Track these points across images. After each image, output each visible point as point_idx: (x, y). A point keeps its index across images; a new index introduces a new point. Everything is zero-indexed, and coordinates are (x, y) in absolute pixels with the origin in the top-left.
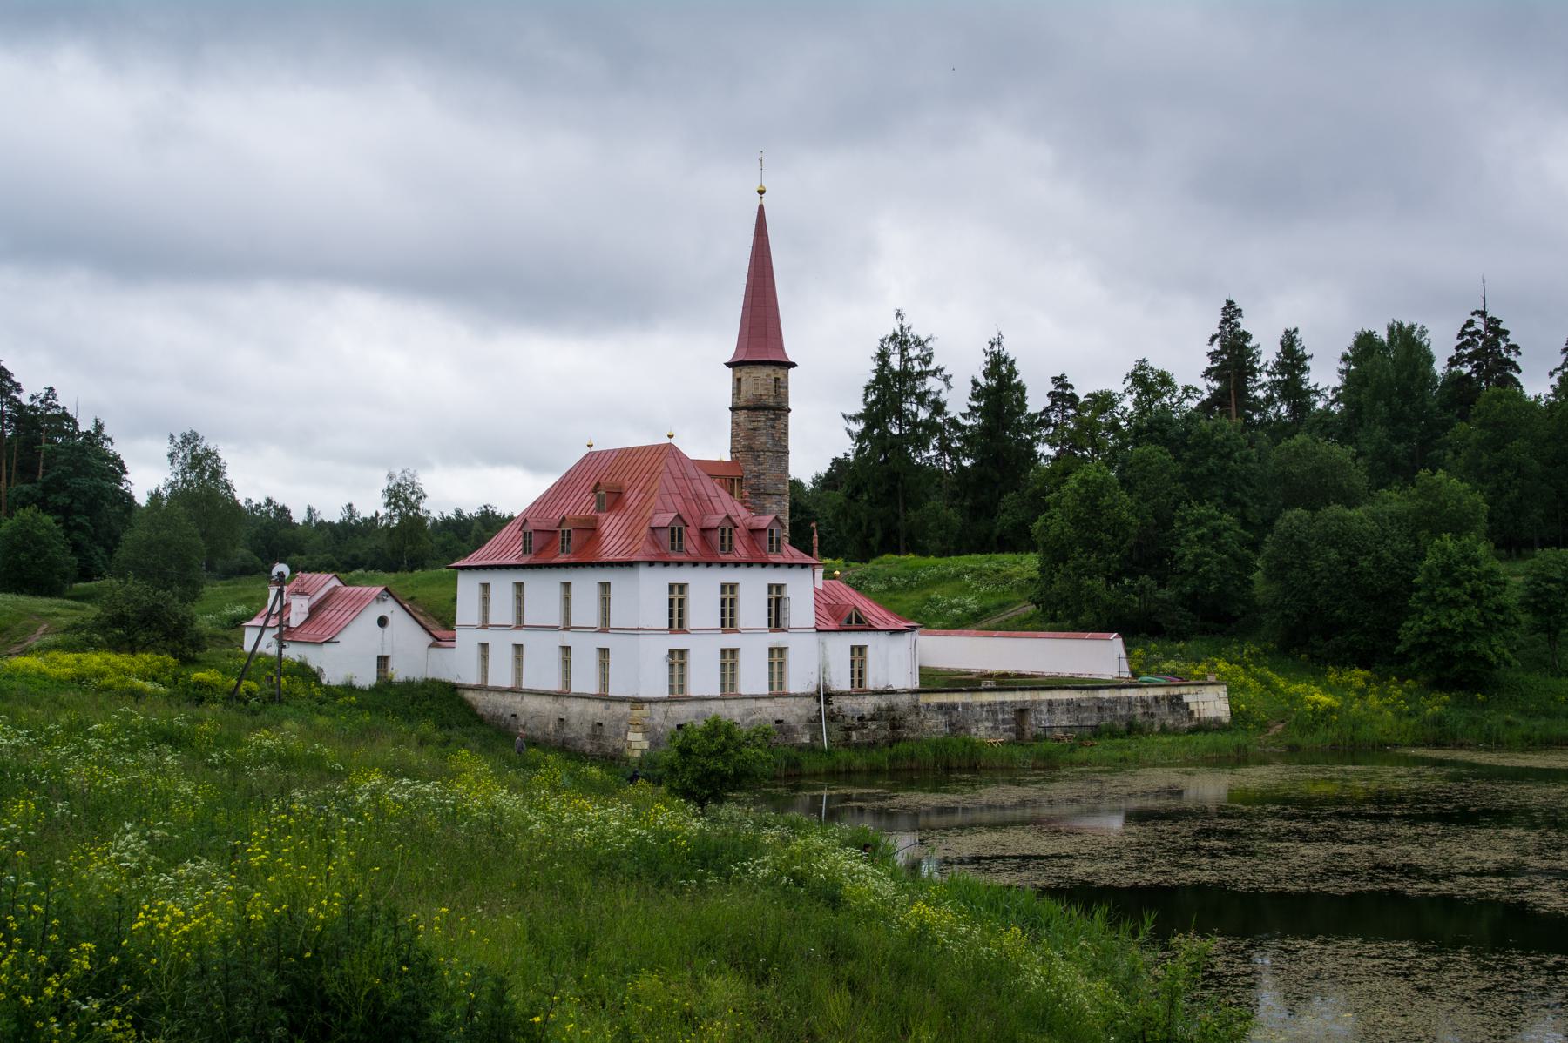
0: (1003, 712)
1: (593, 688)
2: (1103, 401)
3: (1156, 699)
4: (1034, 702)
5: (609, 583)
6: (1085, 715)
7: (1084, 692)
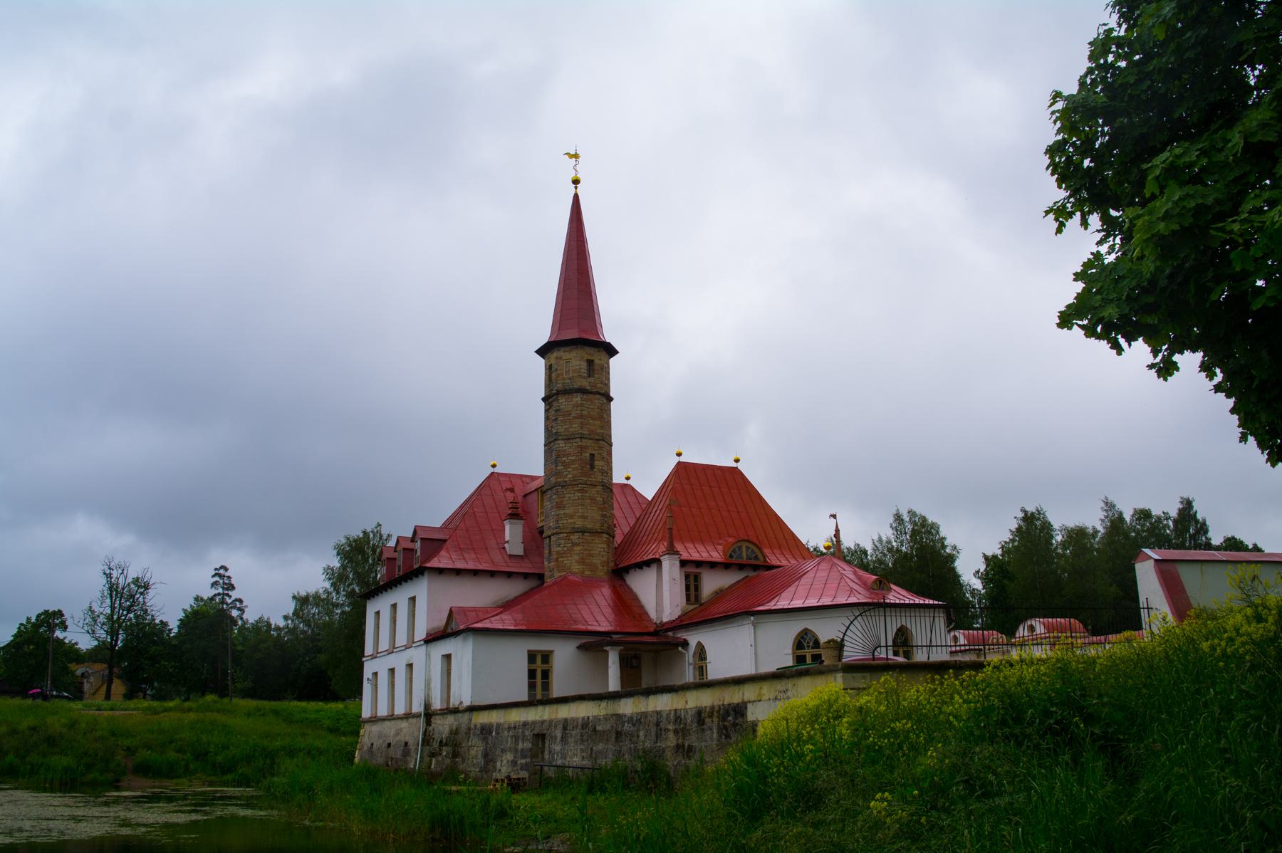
3: (700, 715)
7: (604, 704)
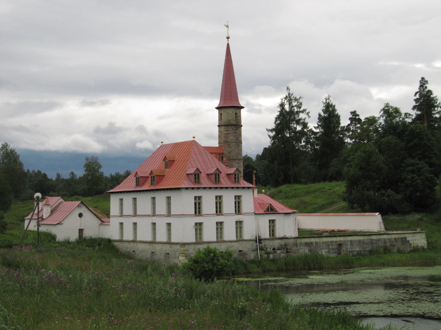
0: (332, 245)
1: (165, 240)
2: (371, 121)
4: (344, 241)
5: (170, 197)
6: (366, 246)
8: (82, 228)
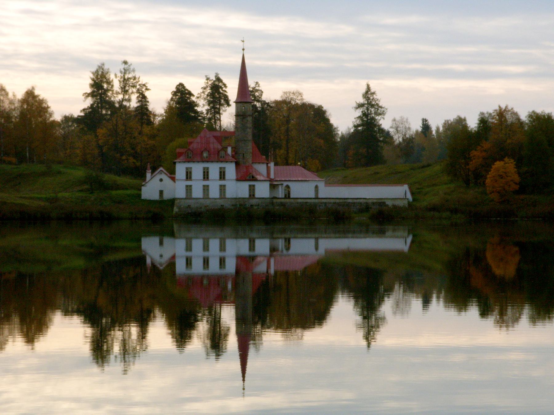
8: (162, 189)
